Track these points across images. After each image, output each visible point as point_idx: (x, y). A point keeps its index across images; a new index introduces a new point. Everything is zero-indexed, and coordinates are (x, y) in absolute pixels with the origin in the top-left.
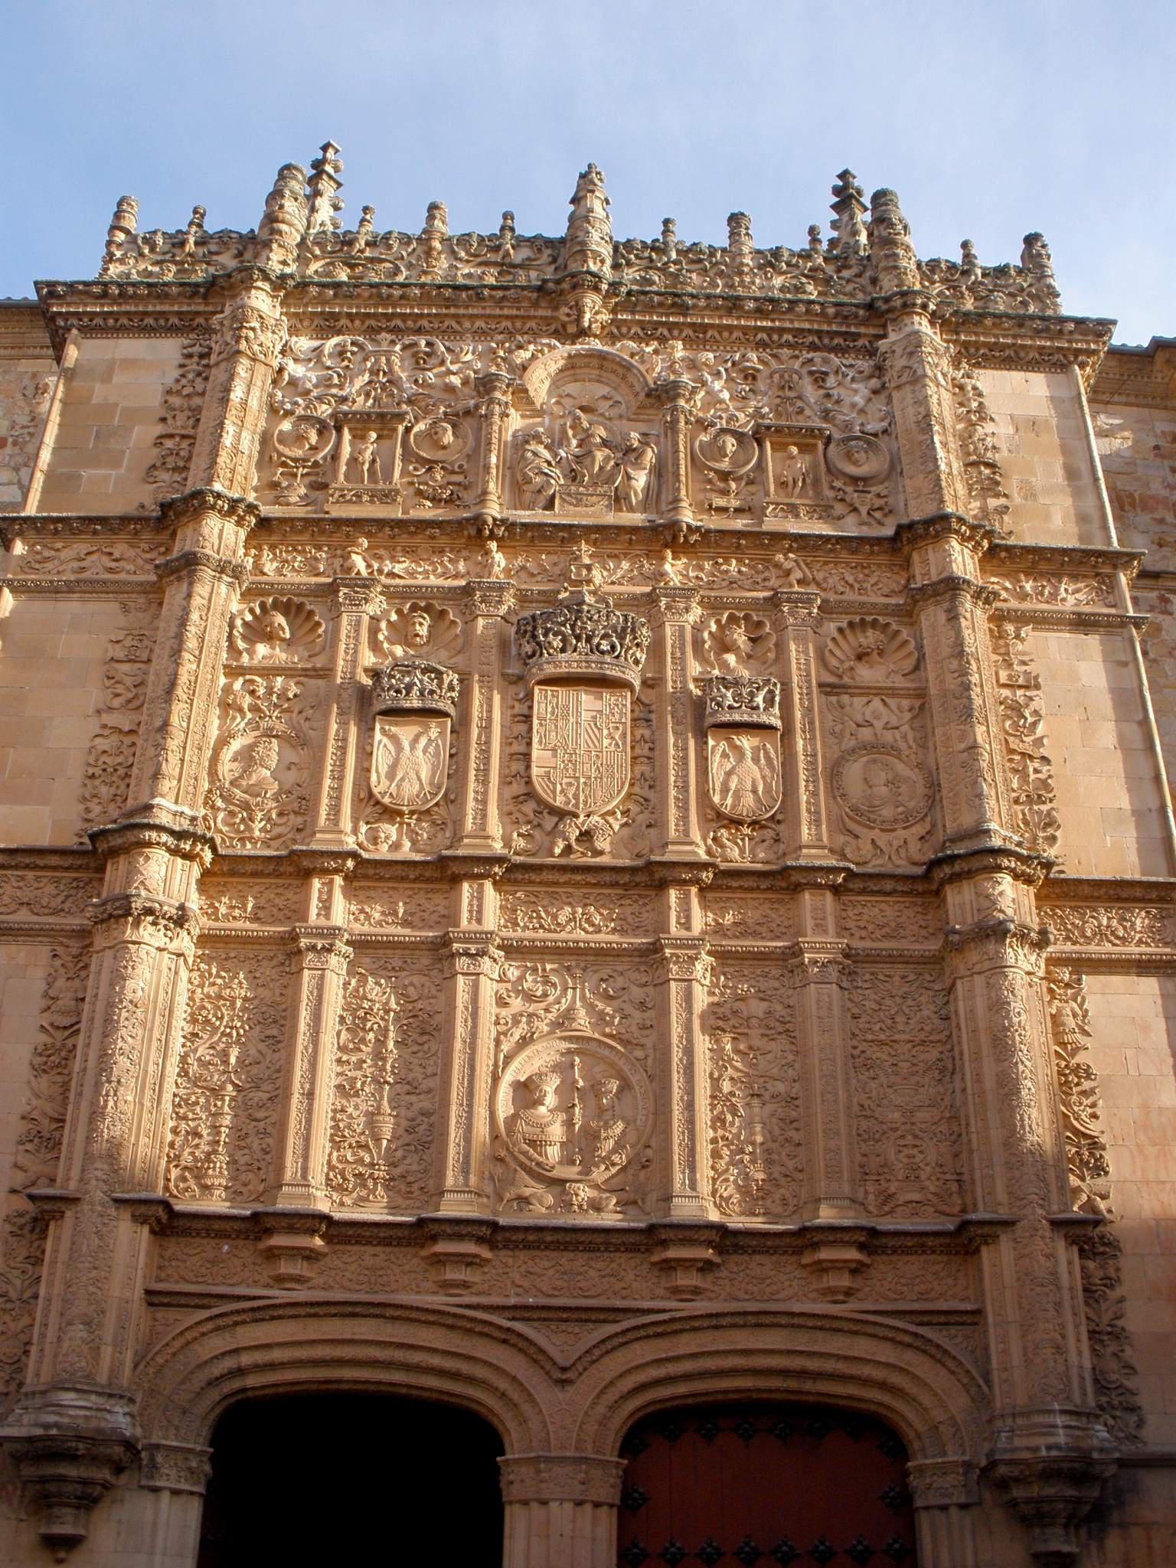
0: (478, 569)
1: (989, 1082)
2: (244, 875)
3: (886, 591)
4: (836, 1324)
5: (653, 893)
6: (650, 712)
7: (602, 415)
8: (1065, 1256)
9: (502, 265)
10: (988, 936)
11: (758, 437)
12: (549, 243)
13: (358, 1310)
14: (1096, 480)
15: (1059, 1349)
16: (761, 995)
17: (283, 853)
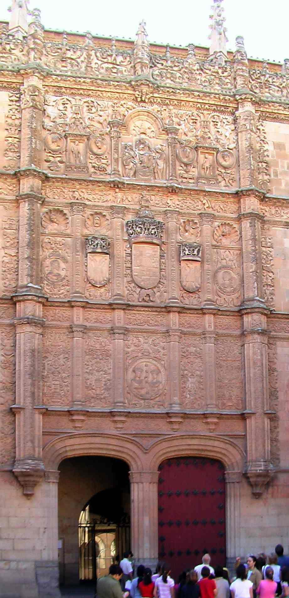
0: (113, 199)
1: (252, 375)
4: (211, 438)
8: (267, 421)
9: (113, 64)
11: (196, 149)
13: (96, 435)
15: (264, 446)
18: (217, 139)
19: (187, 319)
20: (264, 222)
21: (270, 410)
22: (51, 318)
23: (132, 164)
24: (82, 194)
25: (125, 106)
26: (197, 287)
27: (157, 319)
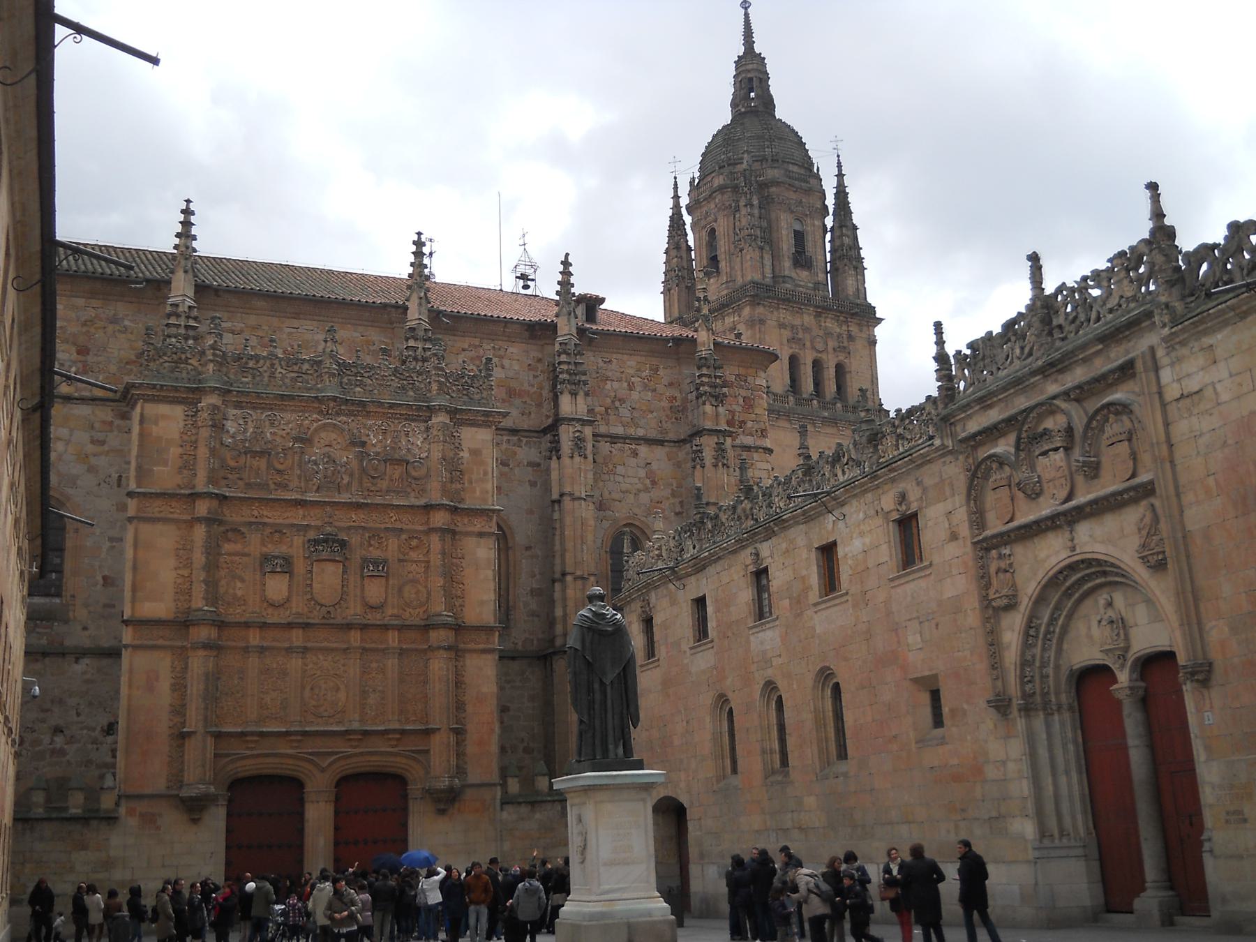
8: (452, 738)
14: (493, 477)
15: (449, 761)
18: (408, 449)
21: (457, 723)
25: (310, 418)
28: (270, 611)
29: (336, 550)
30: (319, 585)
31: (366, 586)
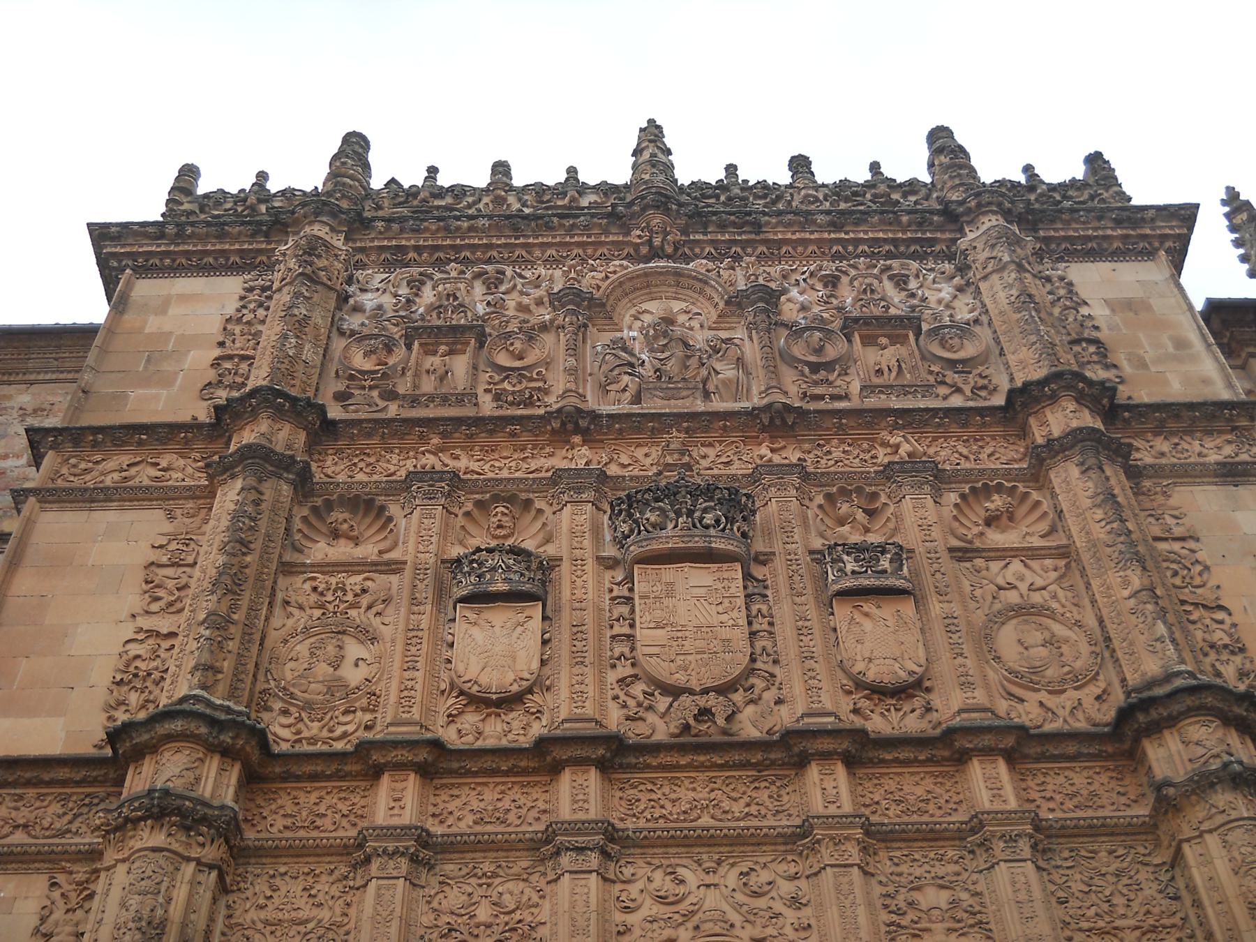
2: (298, 778)
3: (1003, 460)
5: (793, 773)
6: (766, 587)
7: (683, 325)
10: (1212, 785)
12: (615, 189)
16: (940, 882)
17: (350, 748)
19: (890, 784)
20: (1135, 474)
22: (280, 823)
23: (626, 378)
24: (452, 464)
26: (911, 673)
27: (754, 794)
28: (470, 719)
29: (709, 519)
30: (659, 632)
31: (843, 628)
